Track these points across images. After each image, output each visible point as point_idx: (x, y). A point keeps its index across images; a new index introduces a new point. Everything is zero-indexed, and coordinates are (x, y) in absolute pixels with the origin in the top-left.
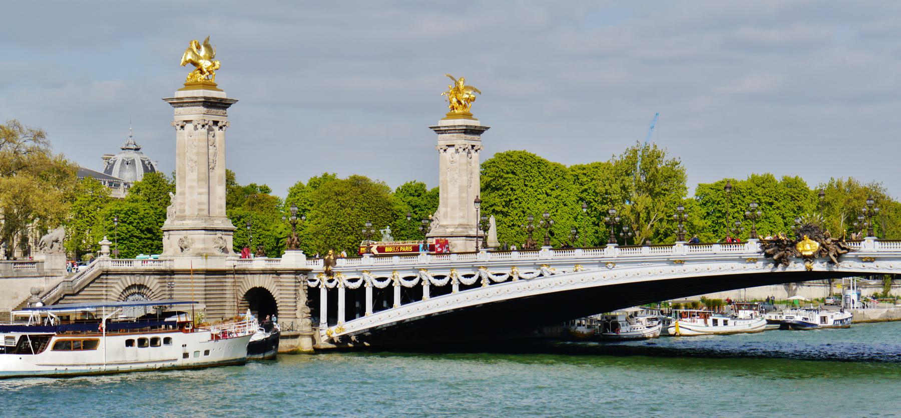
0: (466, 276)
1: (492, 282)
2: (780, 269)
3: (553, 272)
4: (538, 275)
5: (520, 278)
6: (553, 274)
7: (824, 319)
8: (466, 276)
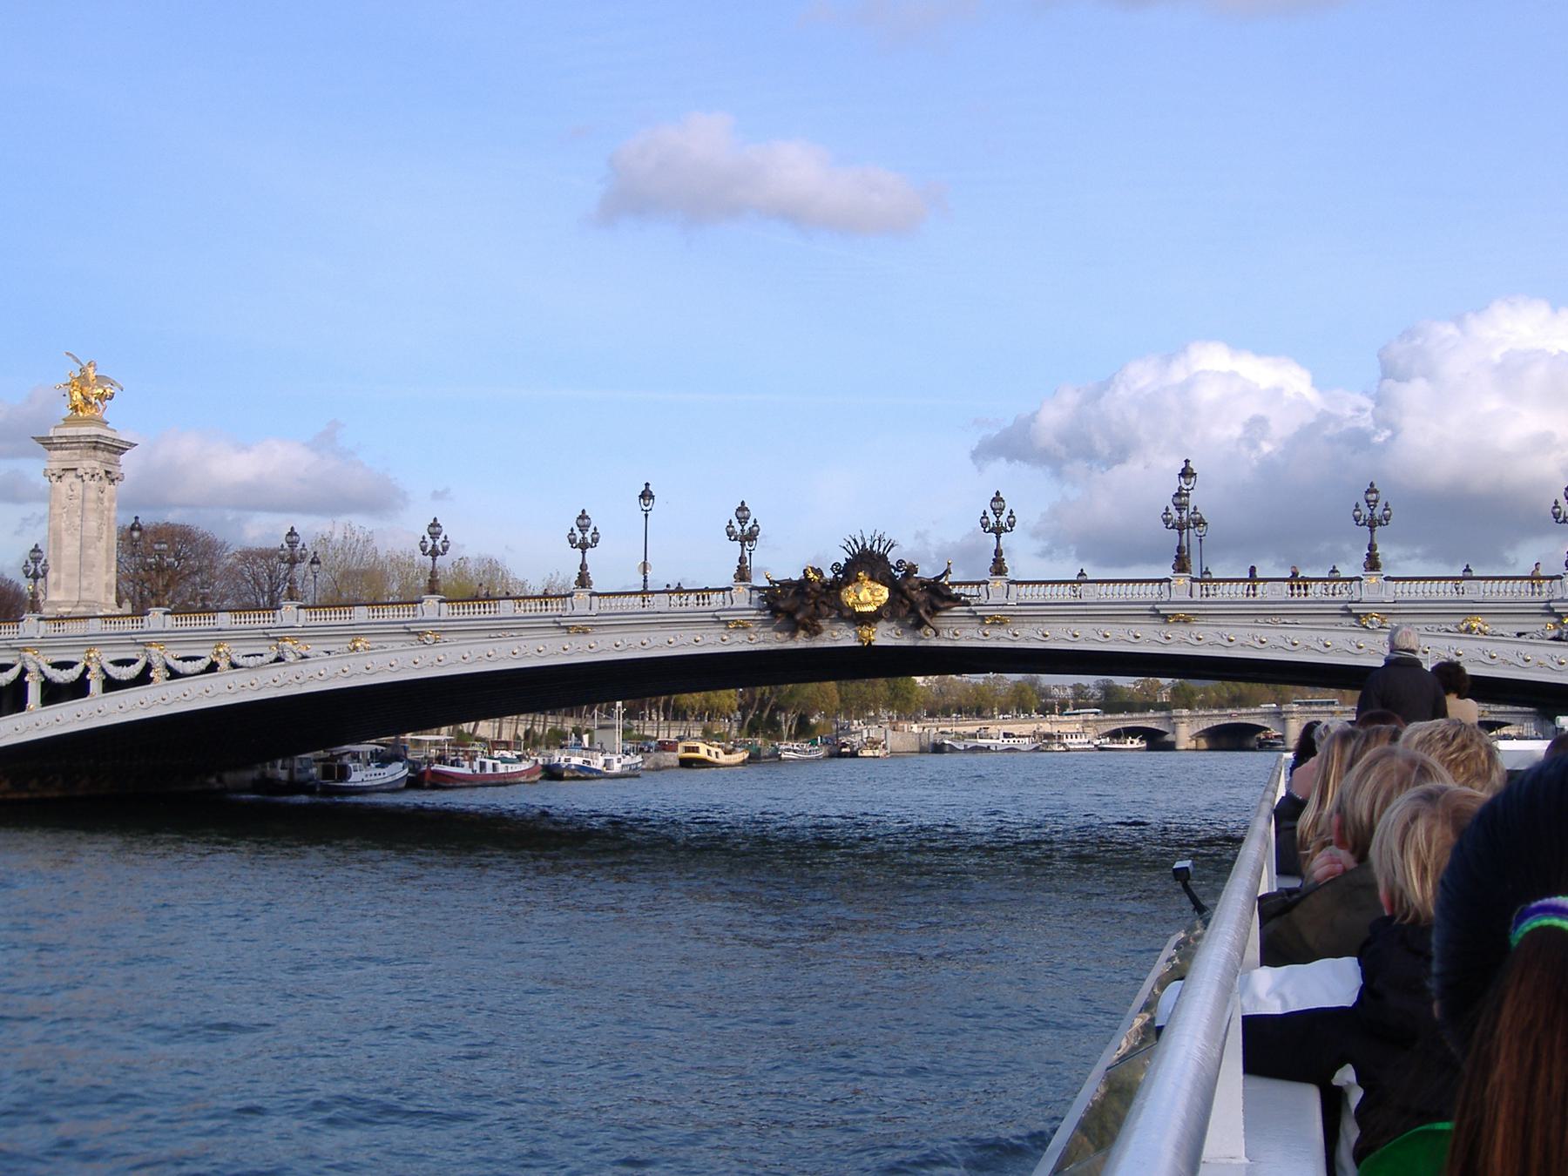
0: (119, 663)
1: (174, 675)
2: (801, 642)
3: (304, 652)
4: (273, 658)
5: (234, 666)
6: (304, 657)
7: (607, 763)
8: (119, 663)
